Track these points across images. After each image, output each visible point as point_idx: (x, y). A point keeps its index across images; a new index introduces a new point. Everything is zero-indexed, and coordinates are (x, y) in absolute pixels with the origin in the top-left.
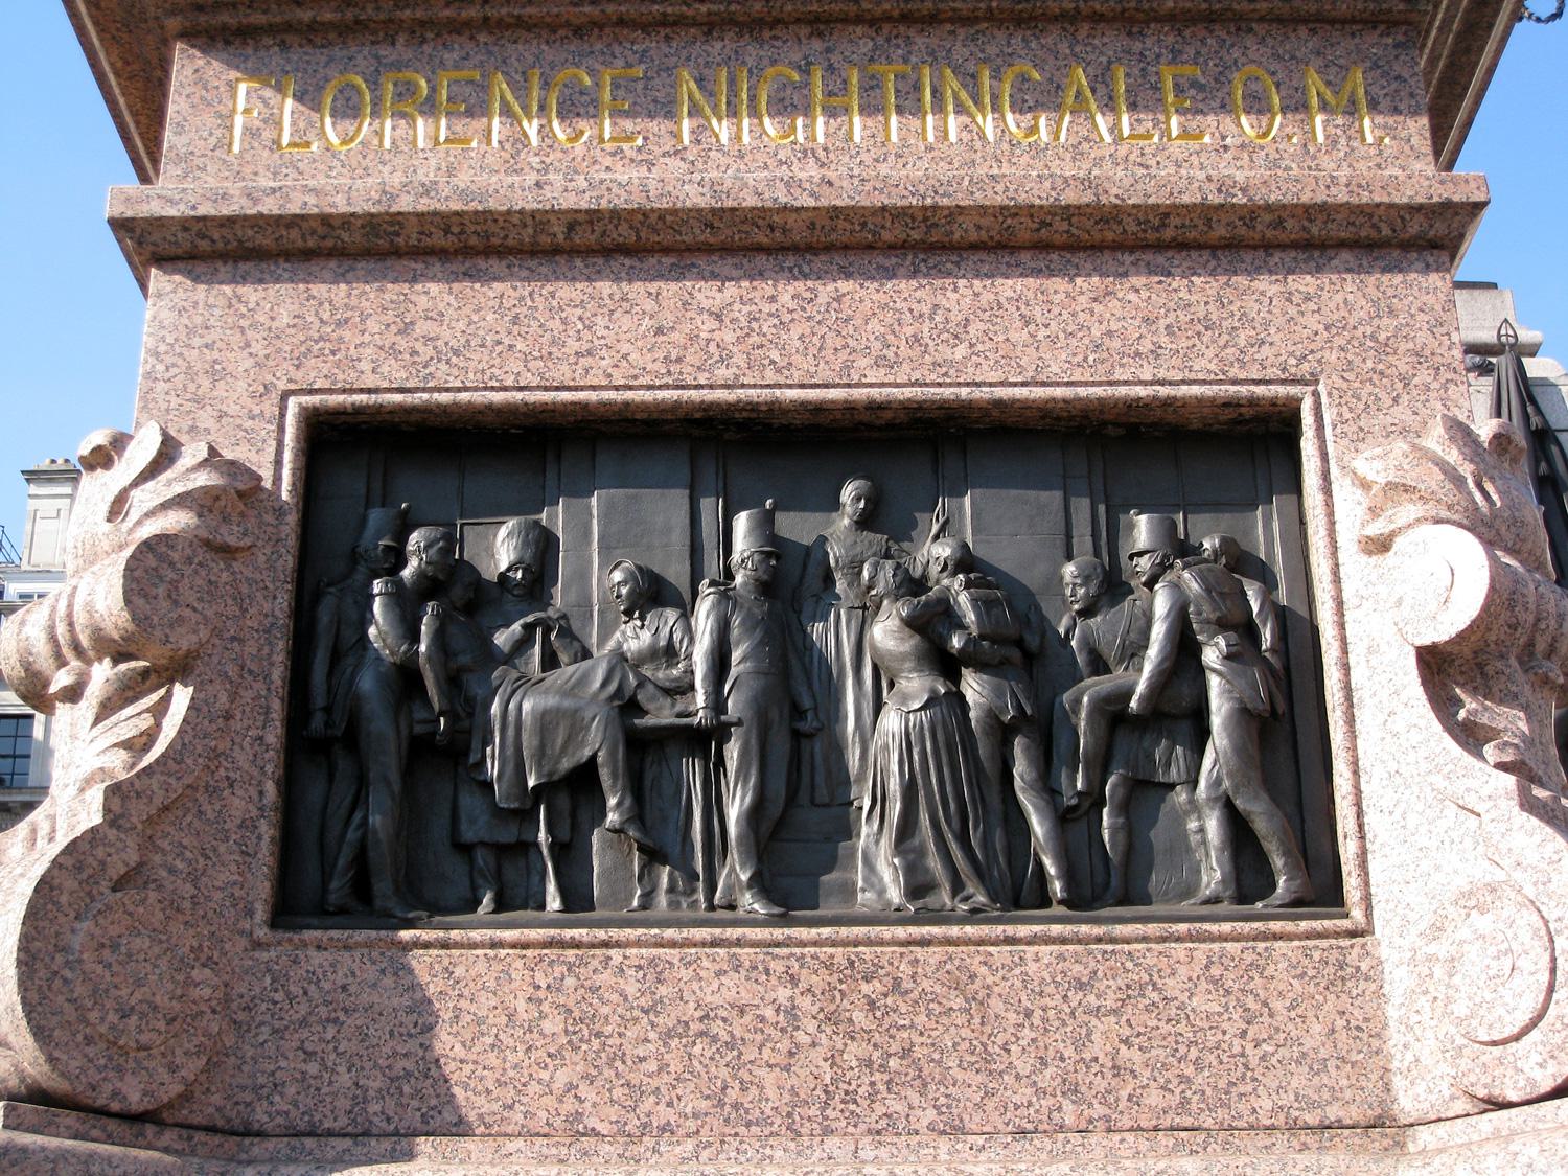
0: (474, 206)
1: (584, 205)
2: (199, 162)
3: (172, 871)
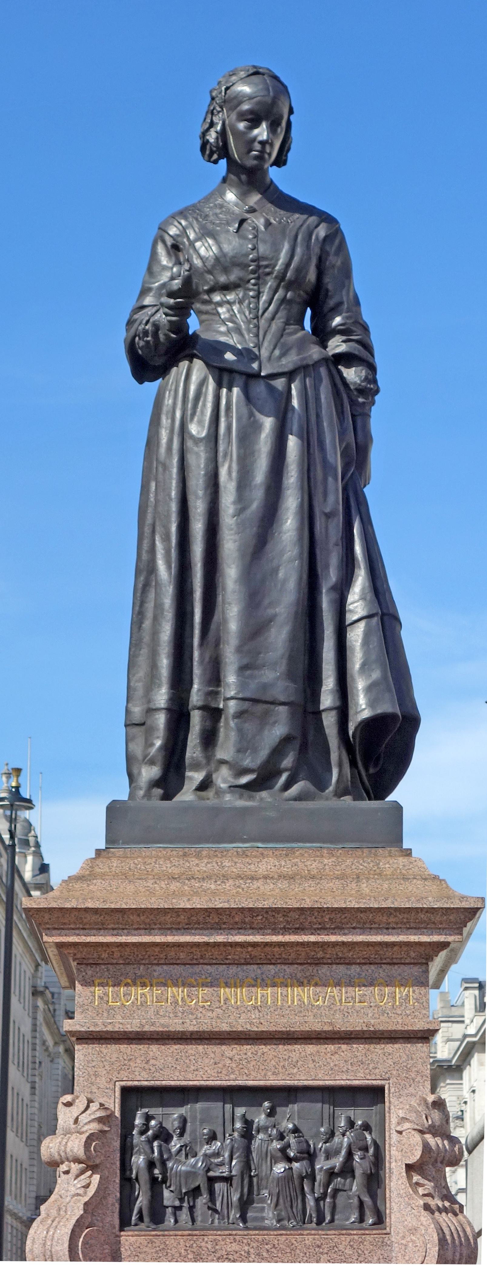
0: (166, 1029)
1: (195, 1029)
2: (86, 1007)
3: (97, 1220)
